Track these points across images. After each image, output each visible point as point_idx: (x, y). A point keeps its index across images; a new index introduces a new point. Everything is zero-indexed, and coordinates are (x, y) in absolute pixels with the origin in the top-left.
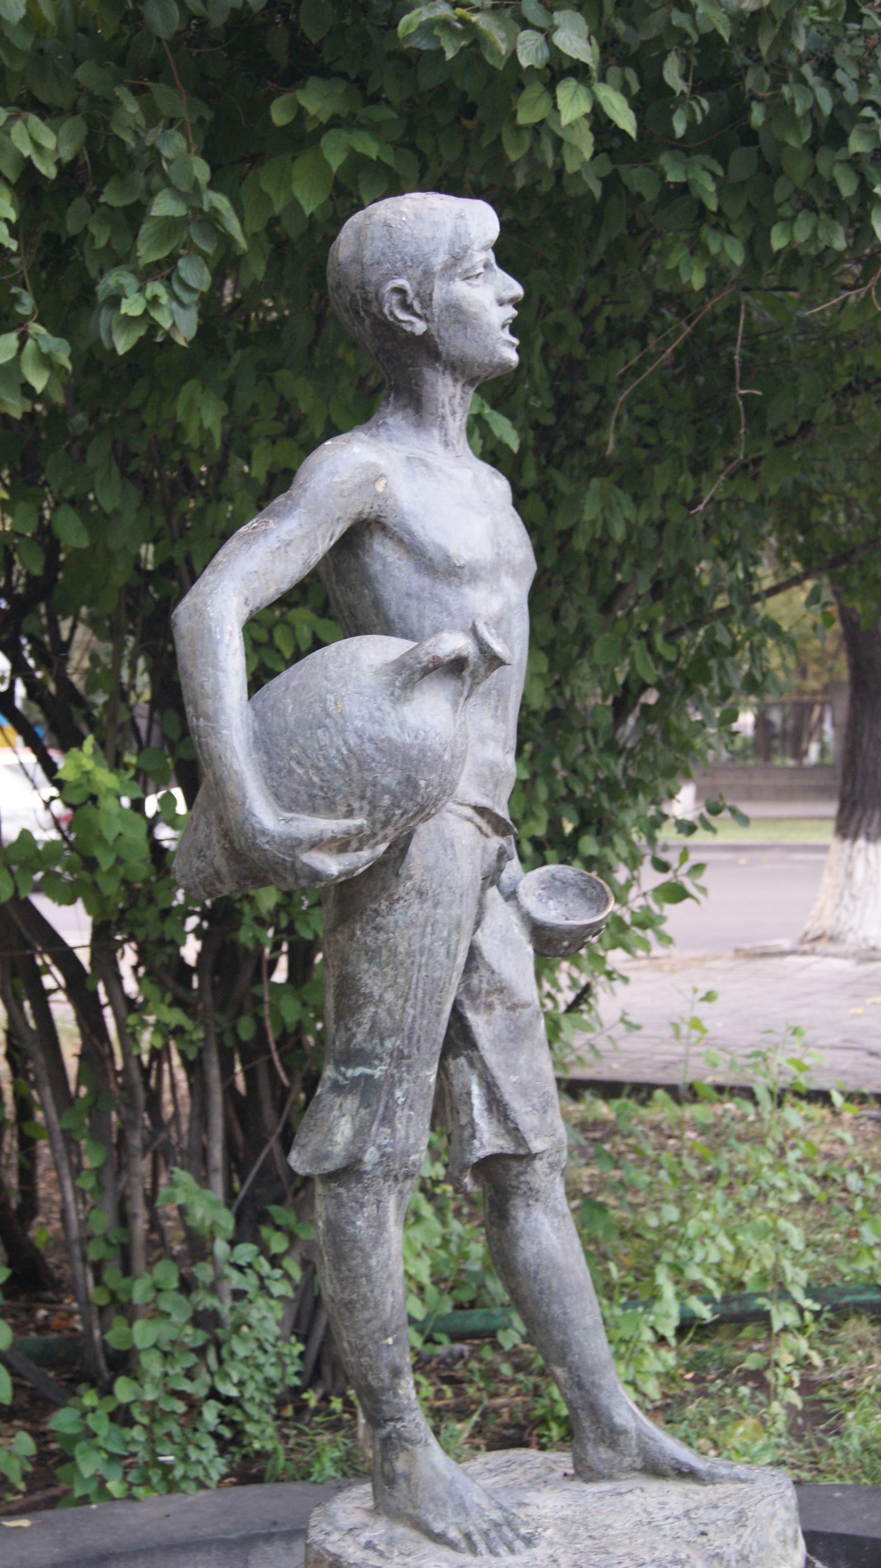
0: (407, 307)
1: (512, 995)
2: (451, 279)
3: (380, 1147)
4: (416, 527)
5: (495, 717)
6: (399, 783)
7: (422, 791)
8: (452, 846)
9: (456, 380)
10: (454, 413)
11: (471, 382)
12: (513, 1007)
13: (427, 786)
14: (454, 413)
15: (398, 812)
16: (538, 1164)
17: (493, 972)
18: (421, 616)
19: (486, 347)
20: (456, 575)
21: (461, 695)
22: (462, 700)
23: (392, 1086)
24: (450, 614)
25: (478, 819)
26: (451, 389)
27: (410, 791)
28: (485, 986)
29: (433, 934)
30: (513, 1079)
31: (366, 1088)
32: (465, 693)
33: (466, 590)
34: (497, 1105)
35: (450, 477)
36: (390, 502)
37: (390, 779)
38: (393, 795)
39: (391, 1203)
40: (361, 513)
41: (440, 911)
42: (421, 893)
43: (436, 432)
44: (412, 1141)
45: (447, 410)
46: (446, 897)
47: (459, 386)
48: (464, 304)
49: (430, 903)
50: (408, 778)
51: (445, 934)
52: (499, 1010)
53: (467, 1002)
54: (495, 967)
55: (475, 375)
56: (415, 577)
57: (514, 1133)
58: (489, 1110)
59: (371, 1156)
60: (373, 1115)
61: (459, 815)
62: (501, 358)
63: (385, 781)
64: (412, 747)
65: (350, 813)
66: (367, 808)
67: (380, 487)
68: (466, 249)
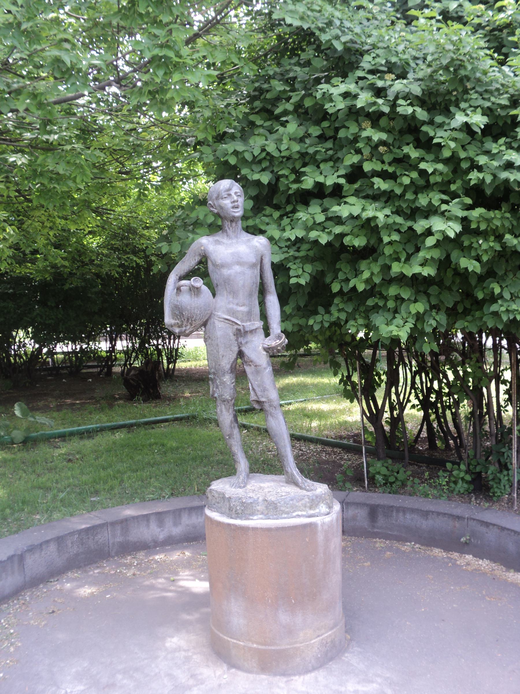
0: (212, 207)
5: (233, 298)
11: (232, 221)
12: (256, 366)
23: (216, 380)
26: (227, 223)
31: (212, 380)
33: (222, 270)
34: (253, 389)
35: (224, 243)
39: (223, 407)
45: (227, 228)
57: (256, 395)
59: (216, 395)
67: (202, 248)
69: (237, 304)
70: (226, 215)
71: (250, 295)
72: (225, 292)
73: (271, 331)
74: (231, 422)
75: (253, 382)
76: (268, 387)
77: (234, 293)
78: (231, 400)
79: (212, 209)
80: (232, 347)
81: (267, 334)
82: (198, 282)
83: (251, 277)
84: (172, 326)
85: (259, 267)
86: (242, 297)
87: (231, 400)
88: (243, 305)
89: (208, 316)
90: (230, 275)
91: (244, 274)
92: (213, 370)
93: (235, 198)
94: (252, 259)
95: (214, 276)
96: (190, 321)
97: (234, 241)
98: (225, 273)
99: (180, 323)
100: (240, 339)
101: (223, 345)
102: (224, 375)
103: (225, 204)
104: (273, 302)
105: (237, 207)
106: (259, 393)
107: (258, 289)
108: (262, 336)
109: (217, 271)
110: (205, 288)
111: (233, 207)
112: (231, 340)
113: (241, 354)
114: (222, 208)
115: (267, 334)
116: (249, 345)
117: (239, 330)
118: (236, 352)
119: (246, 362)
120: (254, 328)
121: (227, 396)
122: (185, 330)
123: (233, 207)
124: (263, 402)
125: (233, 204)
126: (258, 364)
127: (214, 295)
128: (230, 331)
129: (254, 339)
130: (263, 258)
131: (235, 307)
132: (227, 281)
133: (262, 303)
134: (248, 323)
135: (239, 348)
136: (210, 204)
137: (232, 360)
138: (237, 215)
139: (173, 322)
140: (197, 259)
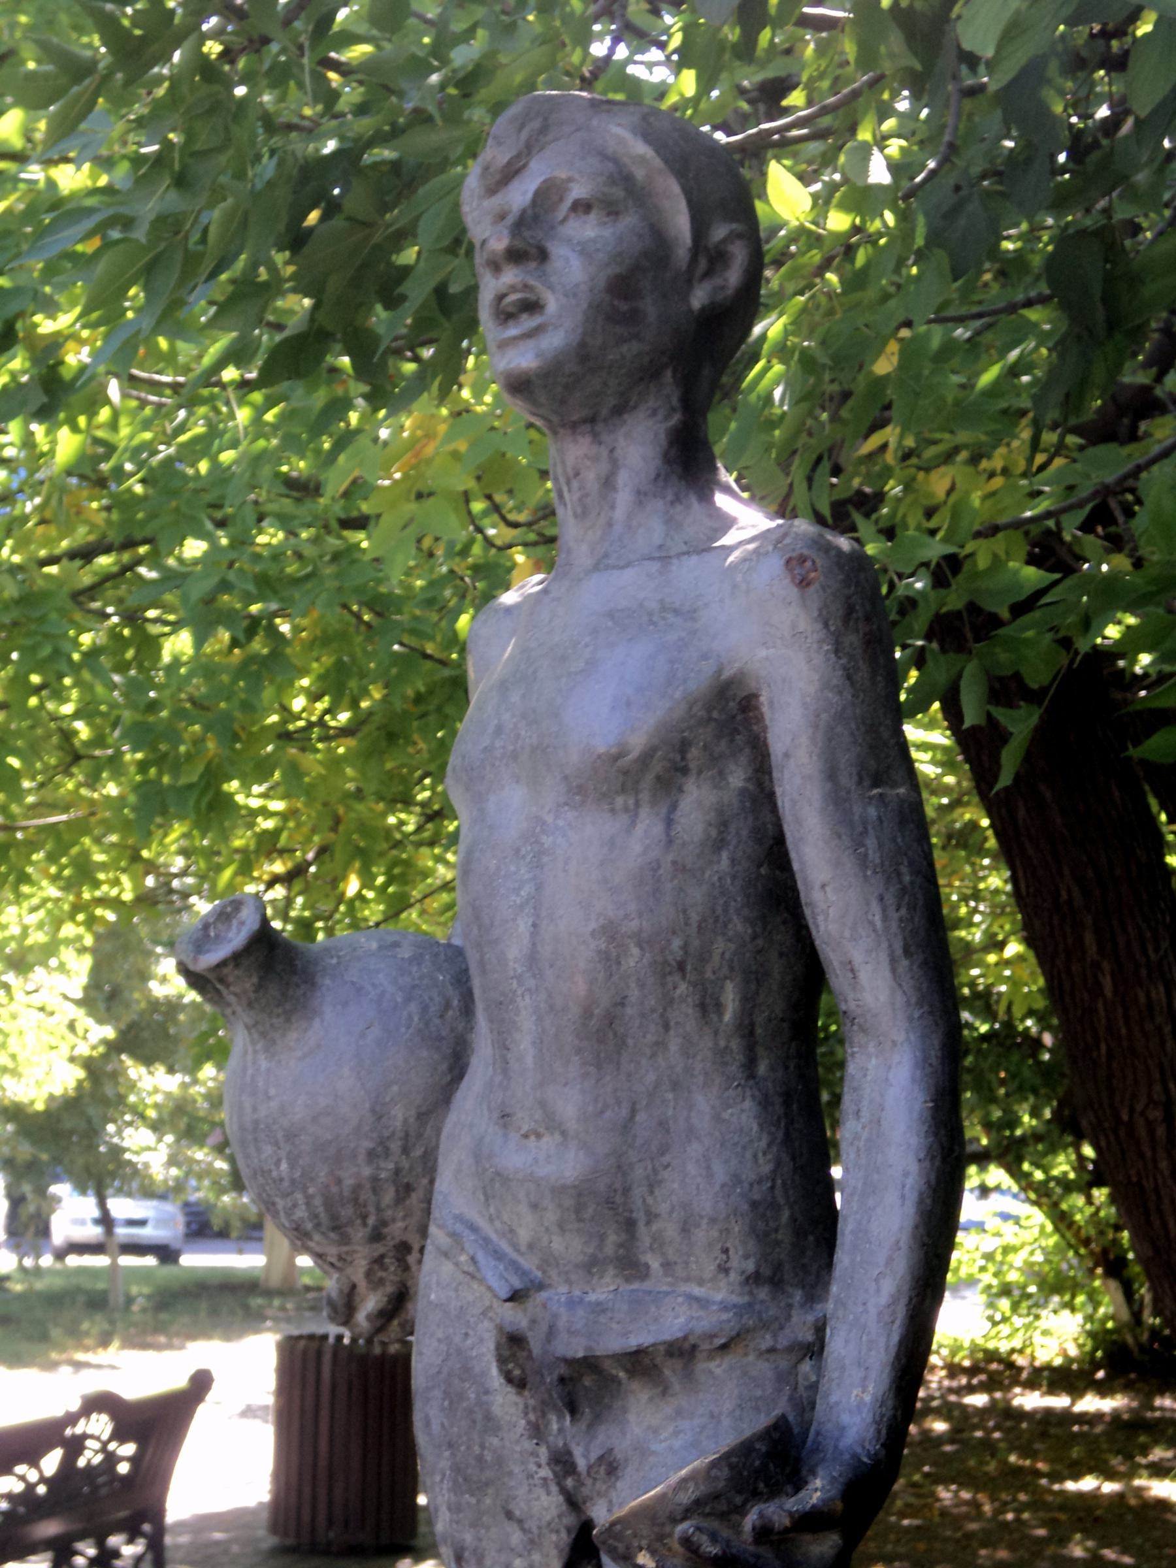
101: (444, 1464)
105: (531, 306)
112: (491, 1424)
135: (573, 1502)
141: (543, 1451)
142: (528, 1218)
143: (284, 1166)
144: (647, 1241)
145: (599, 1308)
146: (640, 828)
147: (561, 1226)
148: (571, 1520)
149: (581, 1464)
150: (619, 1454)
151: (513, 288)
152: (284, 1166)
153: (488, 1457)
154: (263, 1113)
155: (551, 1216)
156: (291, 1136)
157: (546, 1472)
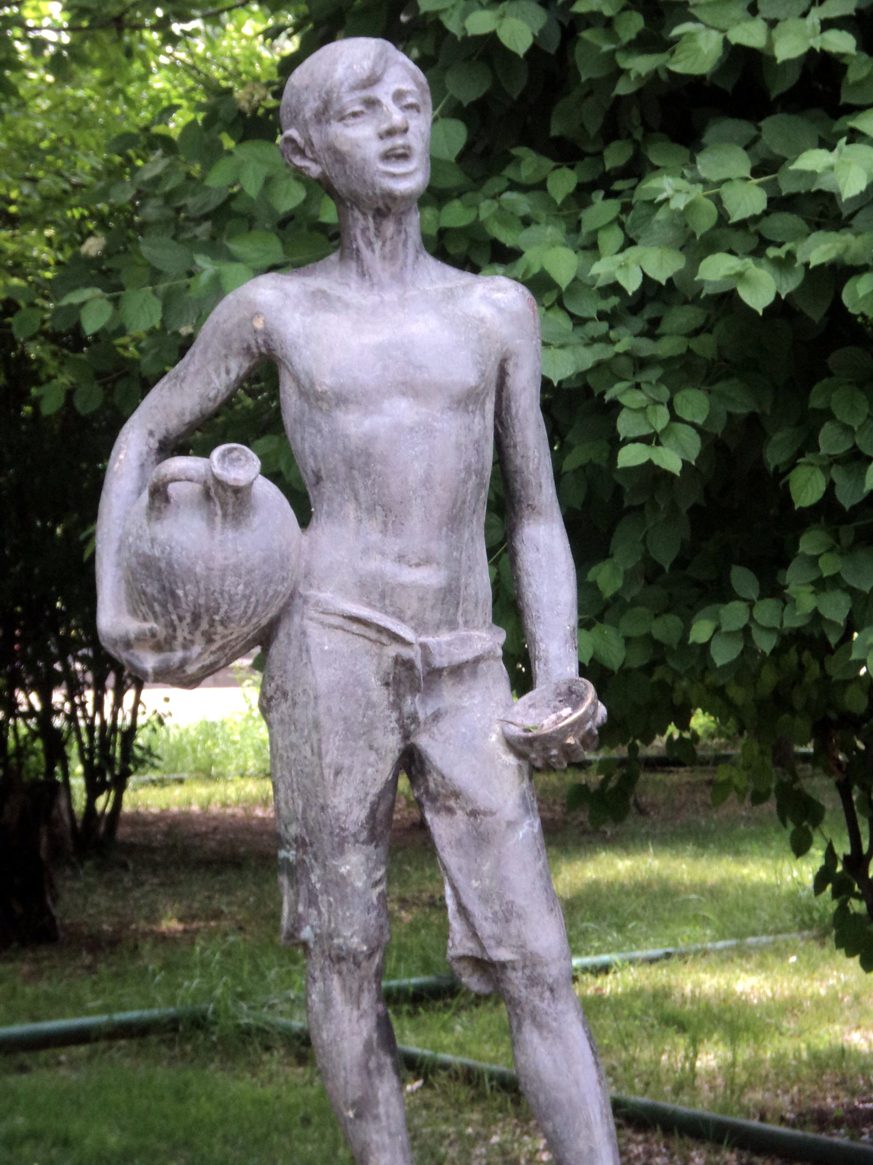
1: (468, 801)
2: (328, 122)
3: (312, 927)
4: (296, 359)
5: (384, 532)
6: (159, 592)
7: (183, 599)
8: (307, 651)
9: (364, 214)
10: (370, 244)
11: (381, 214)
12: (474, 814)
13: (186, 595)
14: (370, 244)
15: (174, 617)
16: (511, 974)
17: (443, 777)
18: (303, 439)
19: (365, 182)
20: (322, 399)
21: (216, 515)
22: (218, 519)
23: (307, 872)
24: (322, 436)
25: (355, 627)
26: (361, 222)
27: (170, 600)
28: (440, 789)
29: (296, 730)
30: (475, 884)
31: (291, 869)
32: (219, 512)
34: (462, 910)
35: (347, 306)
36: (275, 337)
37: (152, 589)
38: (160, 604)
39: (336, 983)
40: (249, 348)
41: (296, 711)
42: (285, 694)
43: (353, 265)
44: (333, 925)
45: (361, 243)
46: (302, 699)
47: (370, 219)
48: (338, 145)
49: (289, 702)
50: (163, 588)
51: (306, 731)
52: (459, 812)
53: (427, 804)
54: (445, 771)
55: (375, 206)
56: (298, 402)
57: (474, 934)
58: (459, 911)
59: (306, 933)
60: (297, 894)
61: (322, 623)
62: (381, 189)
63: (149, 590)
64: (159, 559)
65: (145, 619)
66: (150, 614)
67: (259, 324)
68: (329, 93)
69: (401, 558)
70: (357, 187)
71: (454, 520)
72: (350, 508)
73: (539, 669)
74: (368, 1048)
75: (460, 879)
76: (521, 901)
77: (387, 511)
78: (370, 956)
79: (298, 161)
80: (379, 734)
81: (522, 683)
82: (237, 464)
83: (458, 446)
84: (128, 645)
85: (490, 406)
86: (419, 528)
87: (370, 956)
88: (426, 561)
89: (279, 603)
90: (371, 439)
91: (431, 432)
92: (294, 830)
93: (397, 117)
94: (465, 372)
95: (308, 441)
96: (204, 625)
97: (391, 296)
98: (352, 430)
99: (162, 632)
100: (410, 703)
101: (340, 727)
102: (340, 849)
103: (356, 144)
104: (546, 547)
106: (486, 929)
107: (484, 495)
108: (502, 686)
109: (318, 418)
110: (267, 491)
111: (388, 156)
112: (370, 705)
113: (412, 761)
114: (339, 157)
115: (522, 683)
116: (444, 725)
117: (407, 665)
118: (392, 758)
119: (434, 799)
120: (468, 655)
121: (352, 938)
122: (184, 662)
123: (388, 156)
124: (503, 965)
125: (388, 144)
126: (481, 805)
127: (305, 517)
128: (370, 667)
129: (466, 702)
130: (510, 368)
131: (389, 568)
132: (361, 463)
133: (502, 551)
134: (445, 637)
135: (406, 736)
136: (290, 140)
137: (375, 790)
138: (403, 186)
139: (132, 626)
140: (237, 366)
141: (394, 715)
142: (415, 605)
143: (241, 587)
144: (460, 611)
145: (449, 644)
146: (476, 420)
147: (433, 607)
148: (401, 746)
149: (421, 716)
150: (442, 711)
151: (403, 147)
152: (241, 587)
153: (366, 720)
154: (232, 560)
155: (430, 603)
156: (250, 572)
157: (394, 725)
